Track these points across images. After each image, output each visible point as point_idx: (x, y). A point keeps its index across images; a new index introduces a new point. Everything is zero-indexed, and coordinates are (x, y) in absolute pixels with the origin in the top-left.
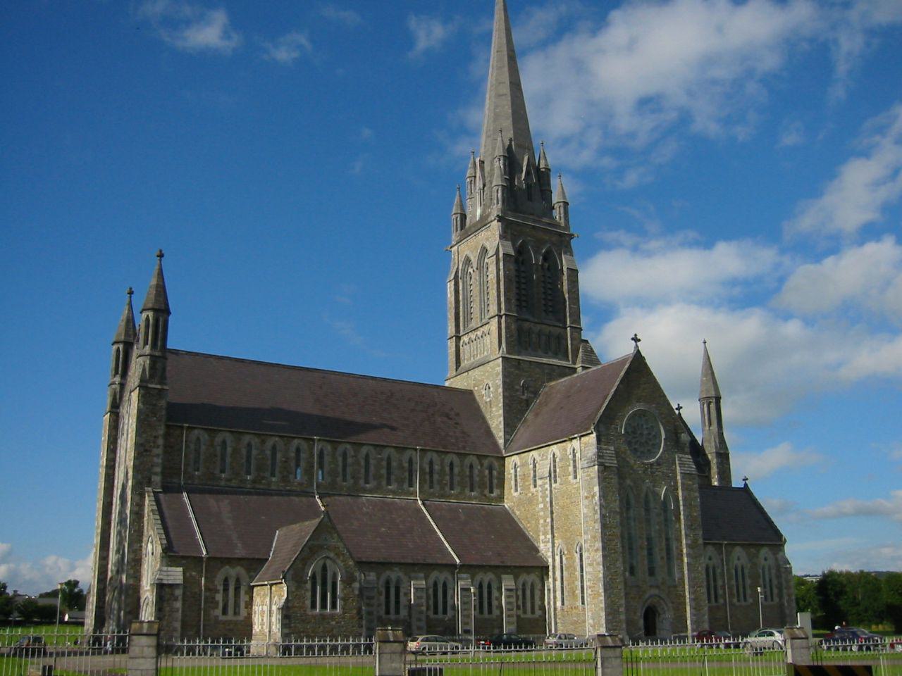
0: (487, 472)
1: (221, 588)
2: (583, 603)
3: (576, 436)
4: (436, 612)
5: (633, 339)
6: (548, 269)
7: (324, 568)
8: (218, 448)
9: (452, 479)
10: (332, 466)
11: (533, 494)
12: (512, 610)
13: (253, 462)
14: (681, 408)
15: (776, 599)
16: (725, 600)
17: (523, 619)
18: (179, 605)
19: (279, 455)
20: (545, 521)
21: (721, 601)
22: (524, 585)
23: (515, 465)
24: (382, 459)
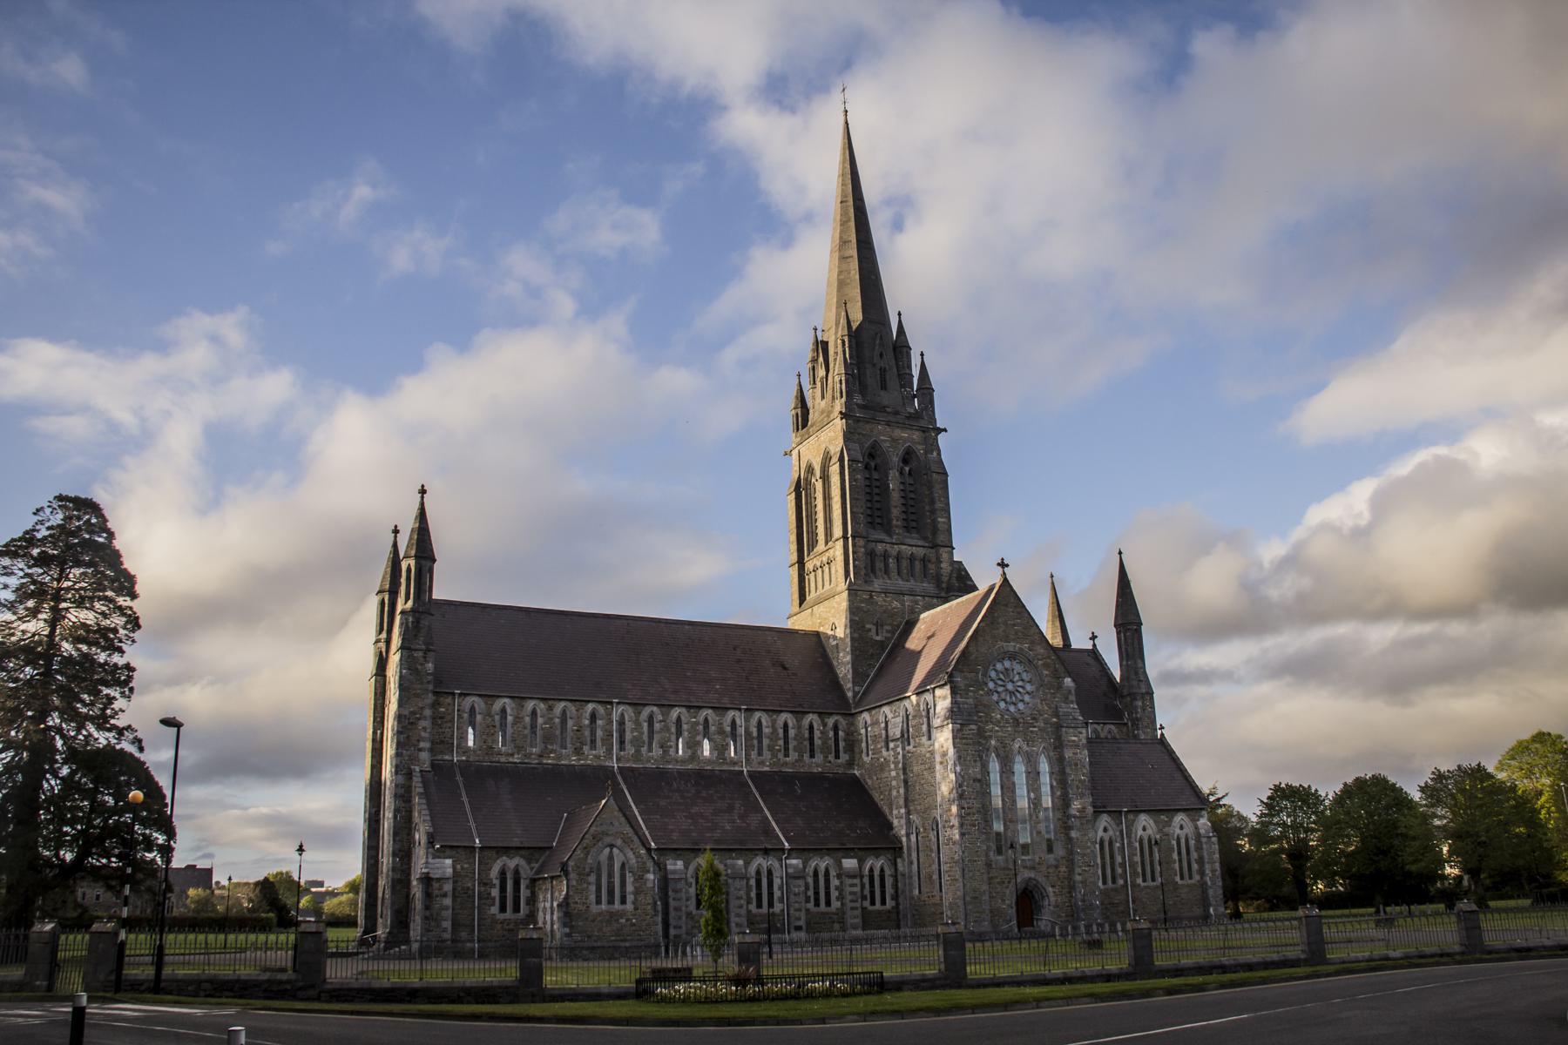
0: (831, 734)
1: (496, 882)
2: (941, 890)
3: (928, 687)
4: (817, 904)
5: (999, 564)
6: (910, 474)
7: (611, 857)
8: (497, 718)
9: (786, 742)
10: (635, 734)
11: (885, 759)
12: (857, 901)
13: (539, 732)
14: (1096, 637)
15: (1197, 877)
16: (1126, 882)
17: (870, 912)
18: (448, 901)
19: (570, 723)
20: (898, 792)
21: (1121, 882)
22: (871, 870)
23: (866, 723)
24: (697, 723)
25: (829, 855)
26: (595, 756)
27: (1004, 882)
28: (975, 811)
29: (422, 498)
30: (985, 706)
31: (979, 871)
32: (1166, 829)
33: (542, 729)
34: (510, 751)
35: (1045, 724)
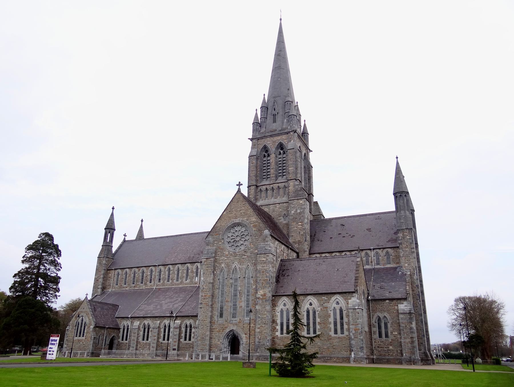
7: (82, 320)
24: (184, 270)
25: (192, 319)
26: (150, 285)
27: (220, 331)
28: (207, 297)
29: (113, 210)
30: (221, 249)
31: (206, 325)
32: (325, 305)
33: (136, 277)
34: (126, 286)
35: (250, 253)
